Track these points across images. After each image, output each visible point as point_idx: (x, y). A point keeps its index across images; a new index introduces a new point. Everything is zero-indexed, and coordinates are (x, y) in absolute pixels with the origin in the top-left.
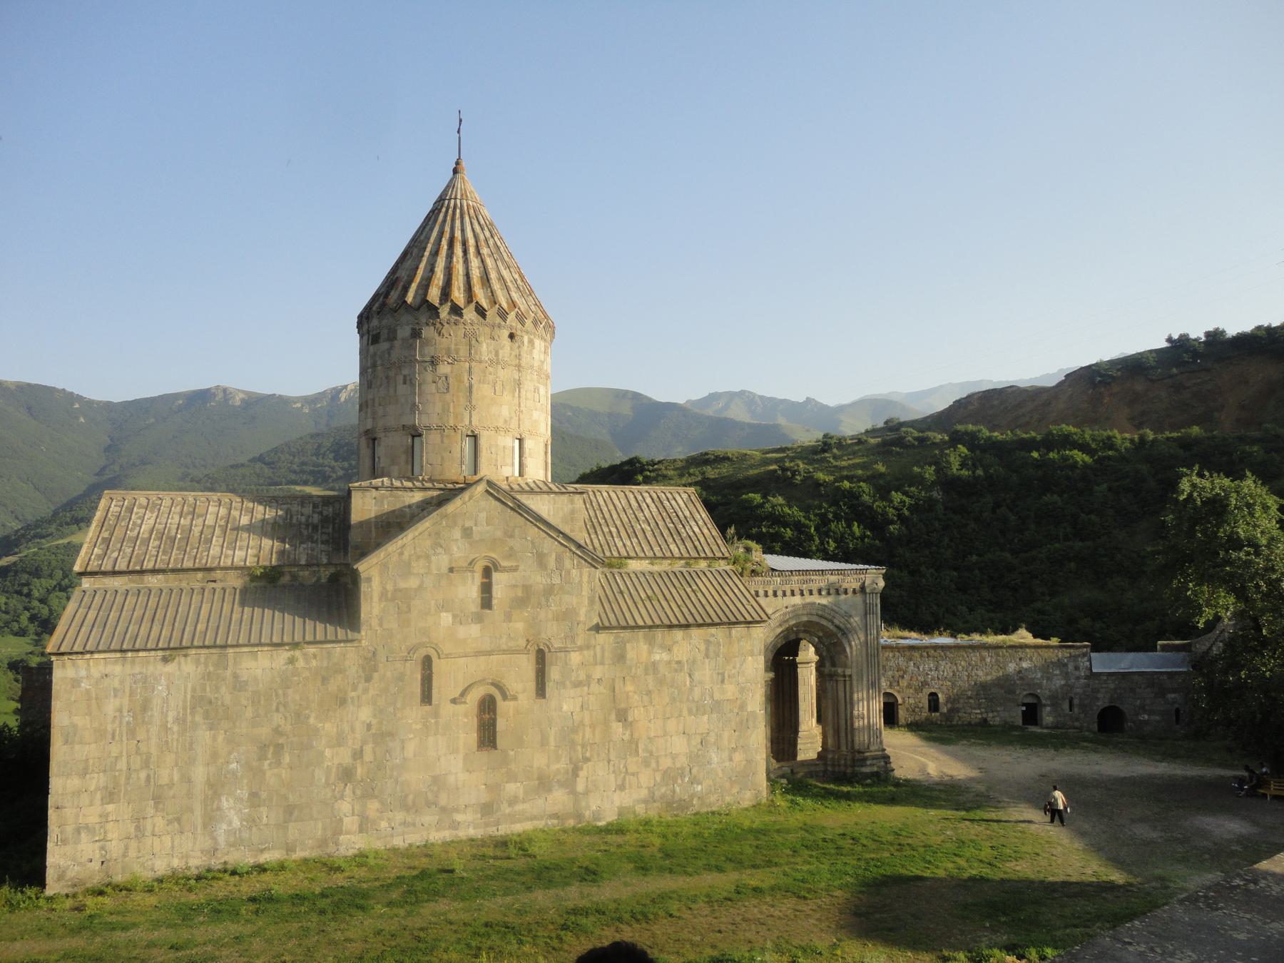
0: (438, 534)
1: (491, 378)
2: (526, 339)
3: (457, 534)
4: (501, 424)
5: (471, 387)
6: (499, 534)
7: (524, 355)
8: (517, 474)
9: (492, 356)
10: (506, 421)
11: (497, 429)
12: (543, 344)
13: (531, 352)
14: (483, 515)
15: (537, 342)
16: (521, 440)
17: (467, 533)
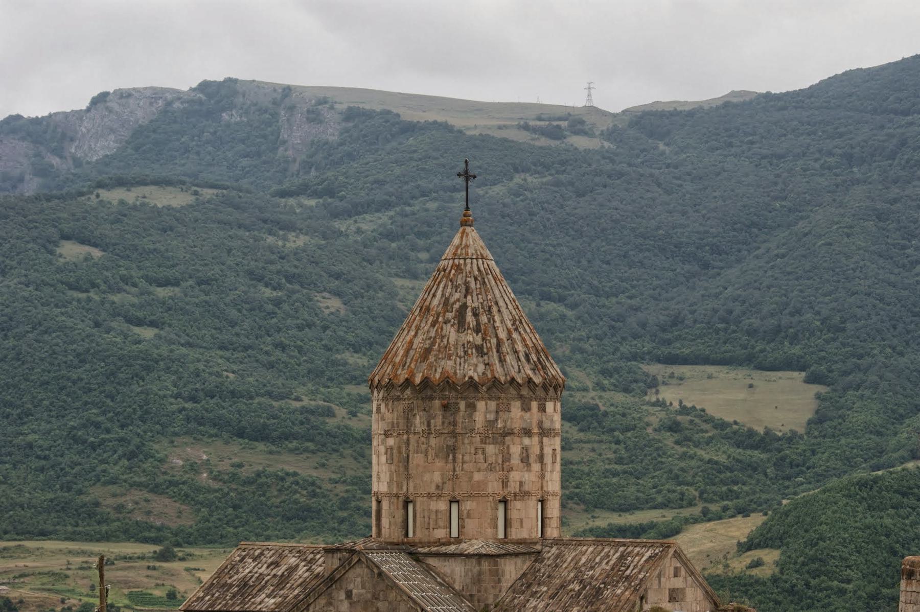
0: (330, 594)
1: (424, 446)
2: (462, 405)
3: (342, 596)
4: (433, 489)
5: (408, 456)
6: (369, 596)
7: (460, 420)
8: (455, 533)
9: (425, 427)
10: (438, 487)
11: (429, 496)
12: (493, 405)
13: (471, 416)
14: (359, 579)
15: (481, 405)
16: (458, 502)
17: (349, 594)
